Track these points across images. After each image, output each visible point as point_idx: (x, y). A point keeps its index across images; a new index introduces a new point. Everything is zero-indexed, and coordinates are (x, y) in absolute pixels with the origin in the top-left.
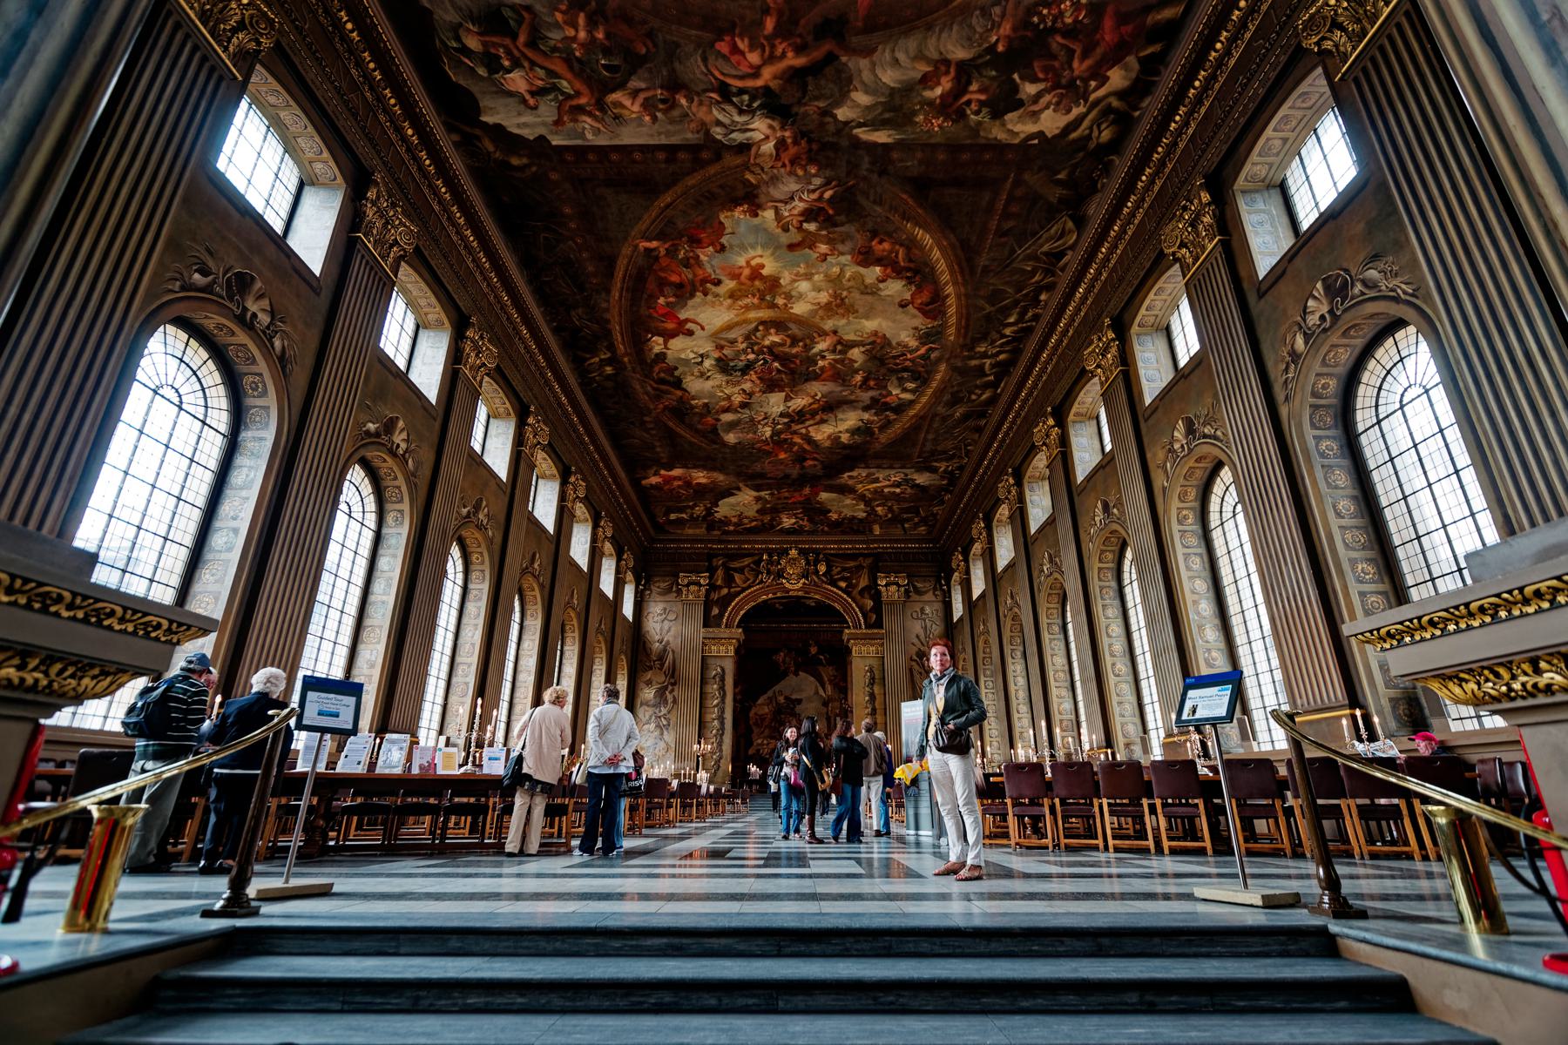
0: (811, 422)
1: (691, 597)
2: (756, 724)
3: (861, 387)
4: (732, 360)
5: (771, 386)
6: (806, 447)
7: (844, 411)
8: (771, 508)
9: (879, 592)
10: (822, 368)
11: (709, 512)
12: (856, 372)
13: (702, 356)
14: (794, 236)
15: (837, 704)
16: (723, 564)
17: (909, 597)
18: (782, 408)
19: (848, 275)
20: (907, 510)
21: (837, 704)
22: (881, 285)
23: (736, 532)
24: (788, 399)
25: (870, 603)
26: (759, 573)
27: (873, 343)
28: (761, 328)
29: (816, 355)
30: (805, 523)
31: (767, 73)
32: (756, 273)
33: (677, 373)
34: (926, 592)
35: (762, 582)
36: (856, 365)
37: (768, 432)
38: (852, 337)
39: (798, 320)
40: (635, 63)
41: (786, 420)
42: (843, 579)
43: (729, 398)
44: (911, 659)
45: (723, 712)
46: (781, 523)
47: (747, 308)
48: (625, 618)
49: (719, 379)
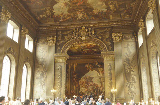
1: (51, 44)
2: (81, 84)
8: (74, 9)
9: (113, 40)
11: (53, 14)
16: (61, 34)
17: (123, 40)
20: (121, 6)
23: (64, 22)
25: (109, 43)
26: (72, 35)
30: (86, 16)
34: (129, 39)
35: (73, 38)
42: (100, 36)
44: (124, 61)
45: (61, 80)
46: (77, 17)
48: (27, 51)
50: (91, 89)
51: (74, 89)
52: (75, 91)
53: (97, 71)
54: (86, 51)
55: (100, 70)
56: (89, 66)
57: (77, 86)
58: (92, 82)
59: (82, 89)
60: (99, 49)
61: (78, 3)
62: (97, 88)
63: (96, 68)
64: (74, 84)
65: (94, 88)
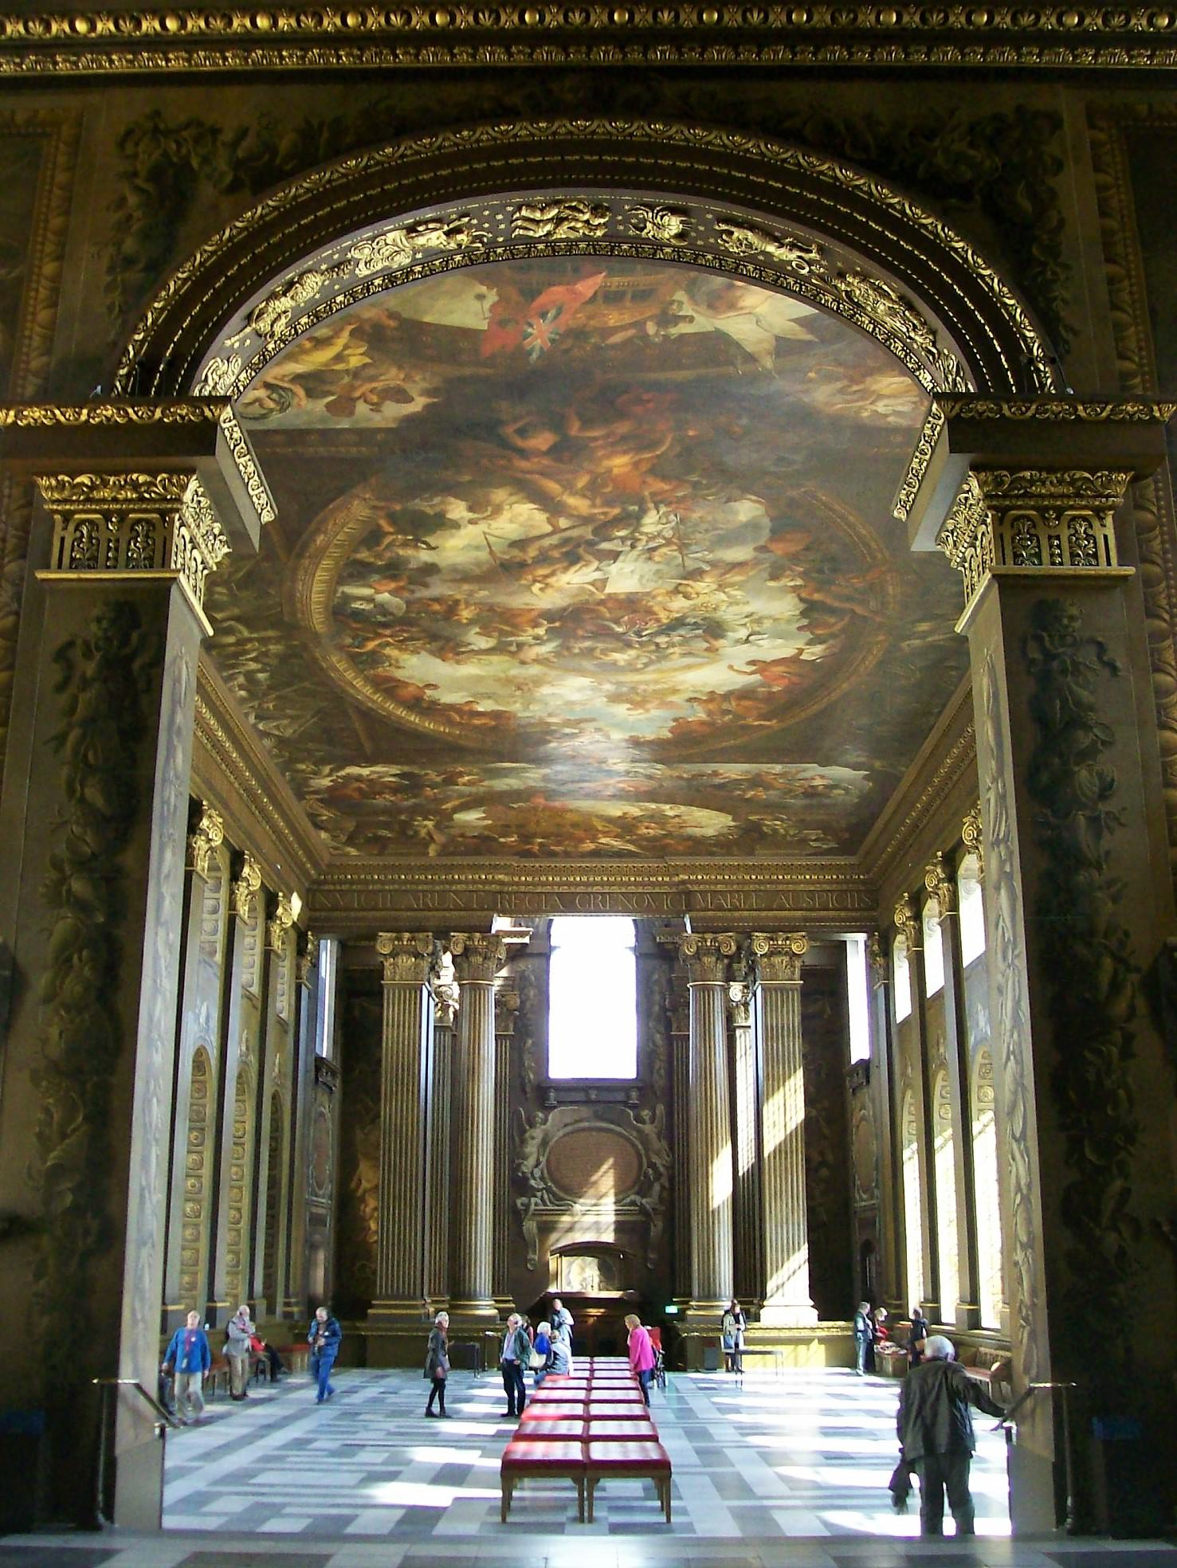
0: (547, 542)
3: (457, 602)
4: (697, 636)
5: (631, 604)
6: (552, 487)
7: (478, 564)
10: (536, 625)
12: (472, 622)
13: (747, 641)
14: (590, 727)
18: (614, 568)
19: (518, 706)
22: (471, 699)
24: (602, 584)
27: (458, 654)
28: (640, 666)
29: (549, 640)
31: (612, 781)
32: (636, 705)
33: (805, 622)
36: (478, 630)
37: (651, 522)
38: (495, 659)
39: (581, 672)
40: (721, 786)
41: (605, 546)
43: (721, 587)
47: (656, 682)
49: (727, 614)
61: (590, 293)
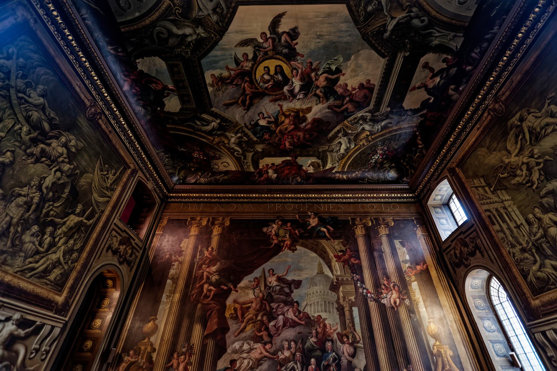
2: (235, 317)
15: (350, 288)
21: (350, 288)
50: (289, 345)
51: (191, 348)
52: (193, 359)
53: (316, 252)
54: (270, 171)
55: (329, 251)
56: (281, 232)
57: (213, 324)
58: (290, 303)
59: (237, 345)
60: (325, 163)
62: (324, 344)
63: (311, 241)
64: (198, 313)
65: (303, 339)
